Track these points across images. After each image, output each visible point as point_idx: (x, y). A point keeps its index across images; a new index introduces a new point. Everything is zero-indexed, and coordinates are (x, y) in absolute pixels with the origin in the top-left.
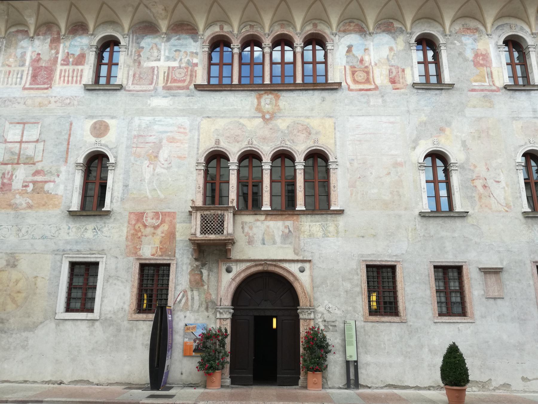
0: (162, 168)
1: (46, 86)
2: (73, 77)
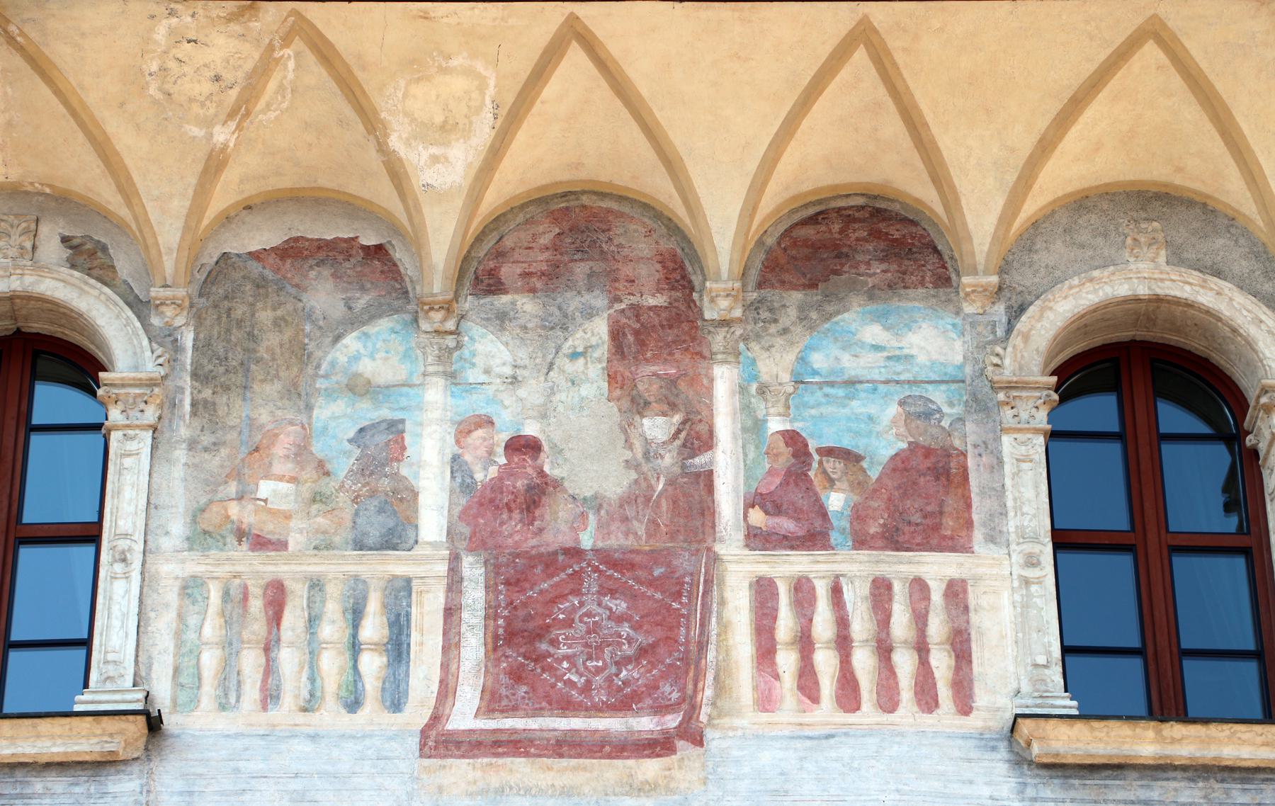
1: (645, 724)
2: (884, 650)
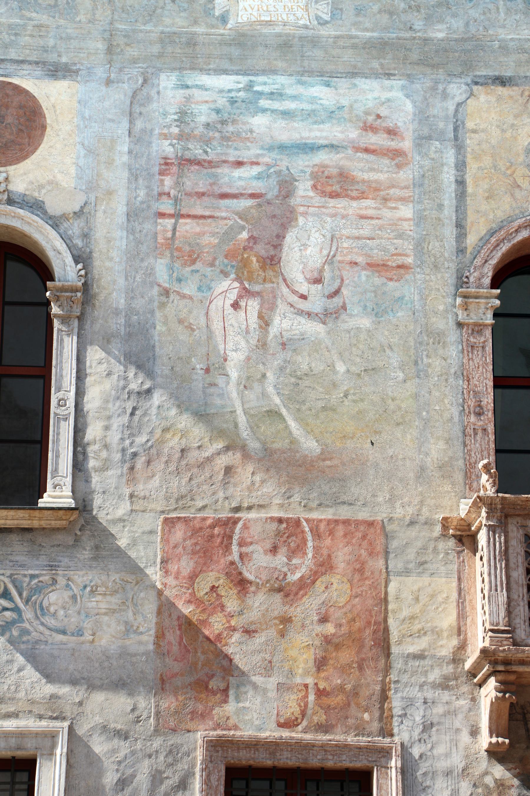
0: (300, 312)
